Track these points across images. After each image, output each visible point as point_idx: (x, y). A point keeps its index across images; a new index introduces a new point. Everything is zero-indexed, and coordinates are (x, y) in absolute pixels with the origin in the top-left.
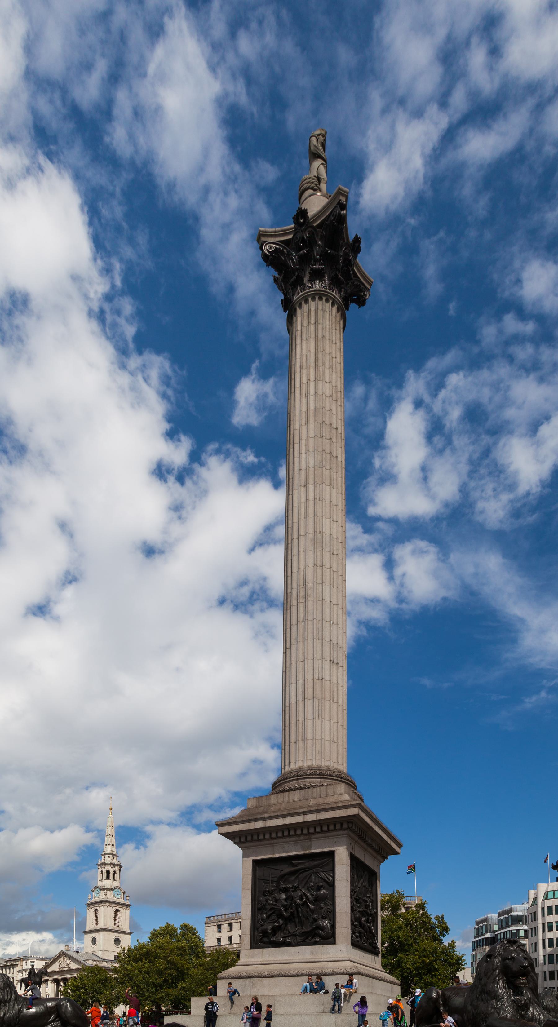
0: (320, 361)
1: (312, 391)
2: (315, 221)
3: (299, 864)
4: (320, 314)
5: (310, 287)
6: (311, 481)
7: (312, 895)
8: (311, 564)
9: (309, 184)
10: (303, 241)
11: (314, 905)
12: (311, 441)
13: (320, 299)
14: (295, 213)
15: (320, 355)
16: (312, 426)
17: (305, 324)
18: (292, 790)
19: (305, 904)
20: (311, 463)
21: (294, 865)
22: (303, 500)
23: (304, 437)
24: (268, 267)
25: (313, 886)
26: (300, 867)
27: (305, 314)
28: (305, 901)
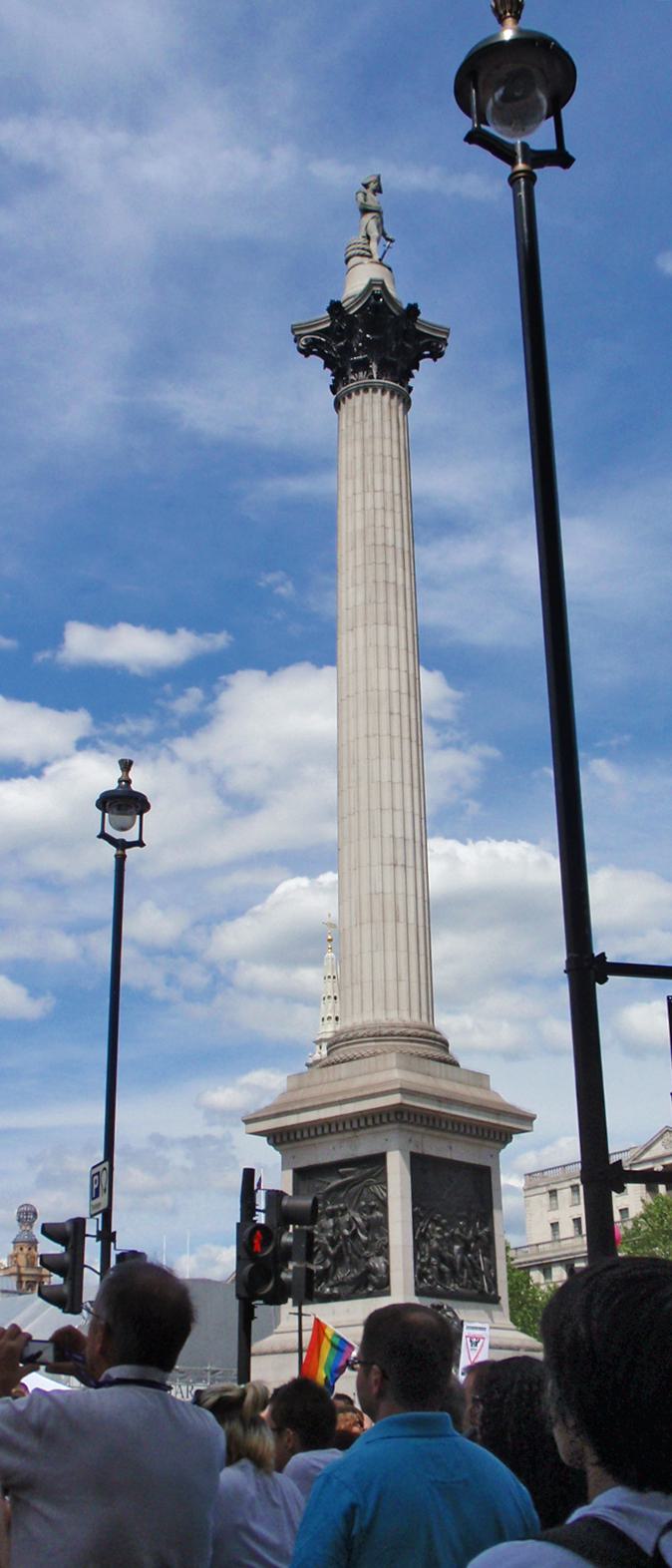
0: (369, 466)
1: (359, 506)
2: (349, 310)
3: (349, 1173)
4: (367, 408)
5: (353, 381)
6: (360, 623)
7: (363, 1220)
8: (362, 734)
9: (358, 251)
10: (341, 330)
11: (367, 1235)
12: (360, 571)
13: (366, 390)
15: (368, 459)
16: (360, 551)
17: (350, 423)
18: (338, 1063)
19: (354, 1235)
20: (360, 598)
21: (343, 1176)
22: (351, 648)
23: (351, 565)
25: (365, 1206)
26: (349, 1178)
27: (350, 410)
28: (356, 1230)
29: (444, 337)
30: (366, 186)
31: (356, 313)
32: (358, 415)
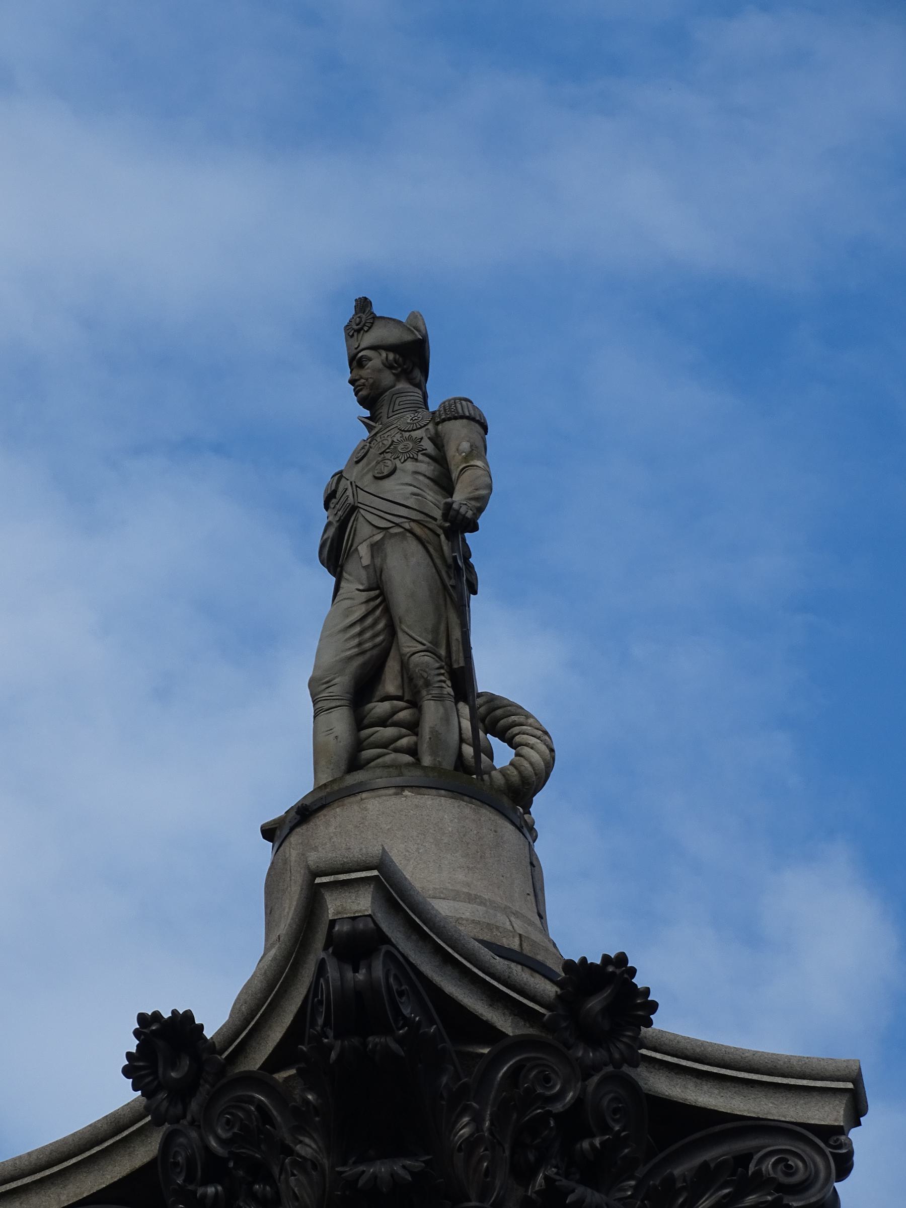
14: (132, 1045)
31: (275, 1062)
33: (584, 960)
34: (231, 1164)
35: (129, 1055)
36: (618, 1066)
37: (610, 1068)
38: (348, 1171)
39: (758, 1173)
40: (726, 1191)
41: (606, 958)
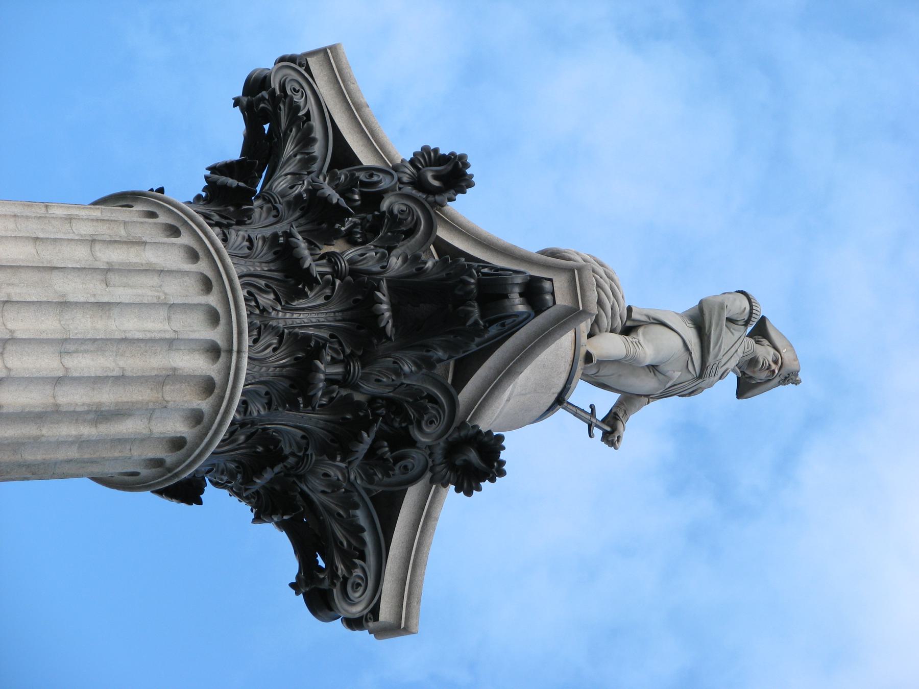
14: (444, 151)
17: (86, 229)
24: (235, 106)
29: (386, 614)
30: (761, 331)
32: (116, 255)
33: (503, 448)
34: (376, 213)
35: (436, 150)
36: (432, 470)
37: (430, 464)
38: (384, 285)
39: (355, 566)
40: (345, 543)
41: (503, 463)
